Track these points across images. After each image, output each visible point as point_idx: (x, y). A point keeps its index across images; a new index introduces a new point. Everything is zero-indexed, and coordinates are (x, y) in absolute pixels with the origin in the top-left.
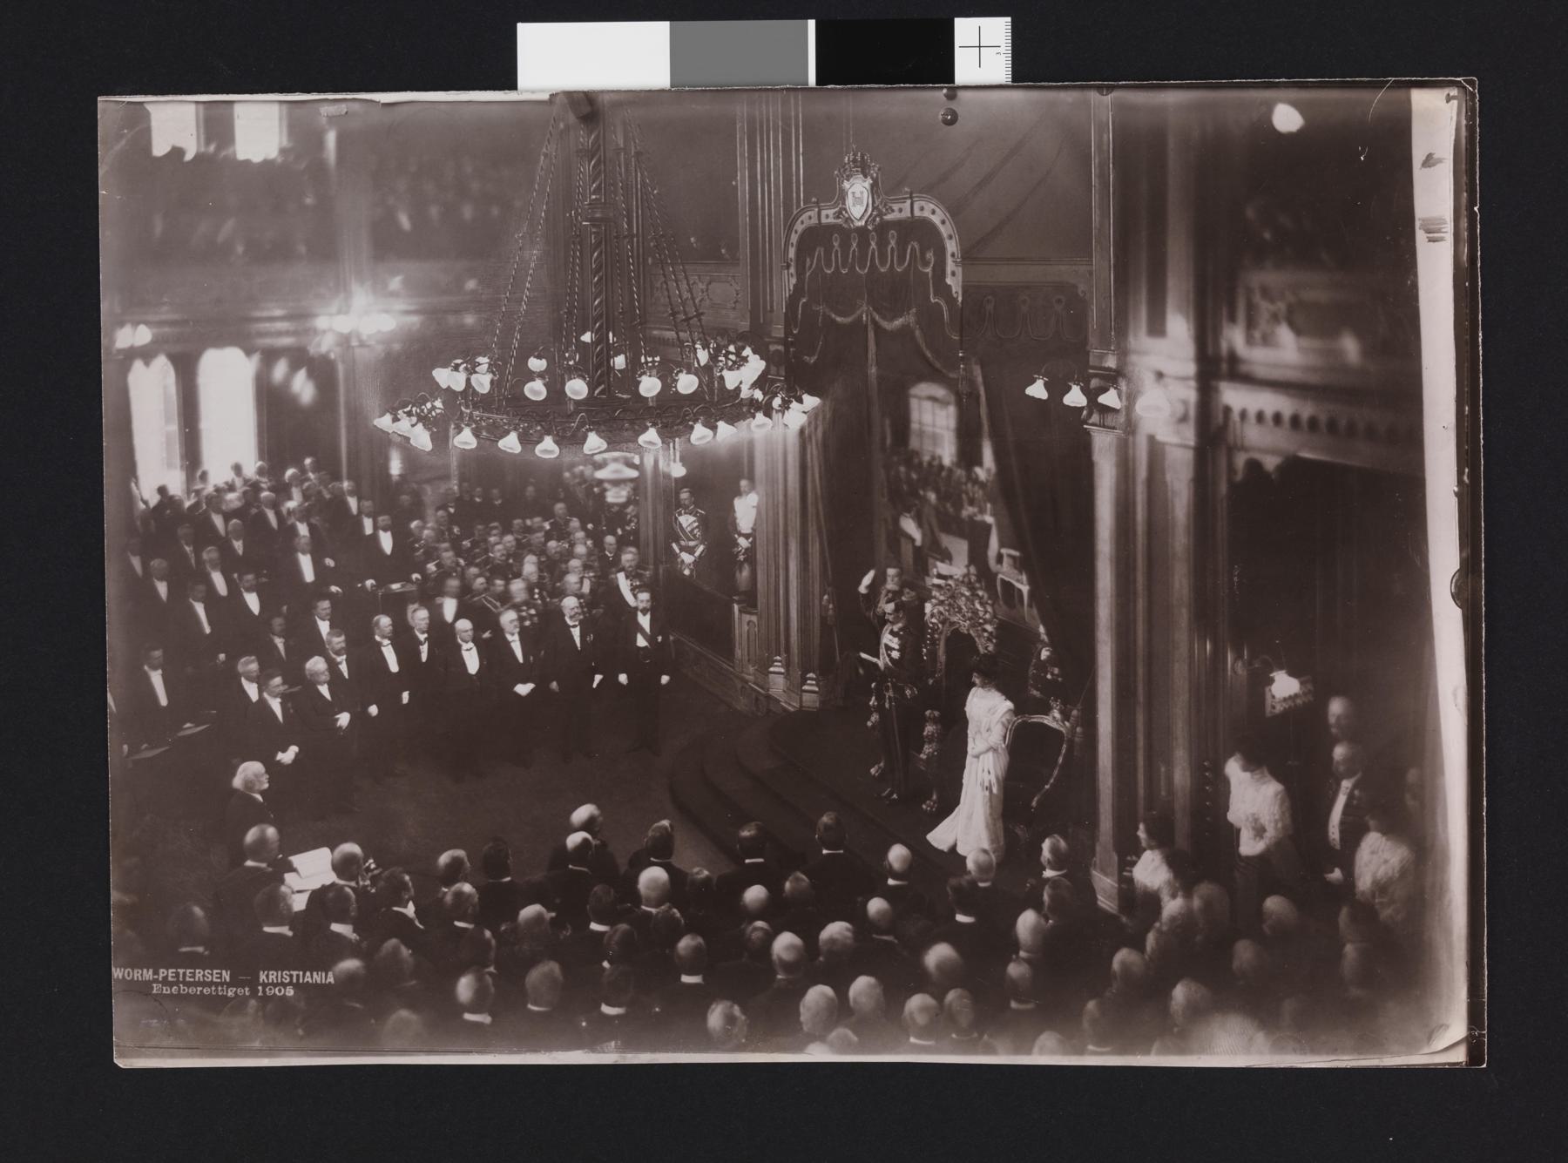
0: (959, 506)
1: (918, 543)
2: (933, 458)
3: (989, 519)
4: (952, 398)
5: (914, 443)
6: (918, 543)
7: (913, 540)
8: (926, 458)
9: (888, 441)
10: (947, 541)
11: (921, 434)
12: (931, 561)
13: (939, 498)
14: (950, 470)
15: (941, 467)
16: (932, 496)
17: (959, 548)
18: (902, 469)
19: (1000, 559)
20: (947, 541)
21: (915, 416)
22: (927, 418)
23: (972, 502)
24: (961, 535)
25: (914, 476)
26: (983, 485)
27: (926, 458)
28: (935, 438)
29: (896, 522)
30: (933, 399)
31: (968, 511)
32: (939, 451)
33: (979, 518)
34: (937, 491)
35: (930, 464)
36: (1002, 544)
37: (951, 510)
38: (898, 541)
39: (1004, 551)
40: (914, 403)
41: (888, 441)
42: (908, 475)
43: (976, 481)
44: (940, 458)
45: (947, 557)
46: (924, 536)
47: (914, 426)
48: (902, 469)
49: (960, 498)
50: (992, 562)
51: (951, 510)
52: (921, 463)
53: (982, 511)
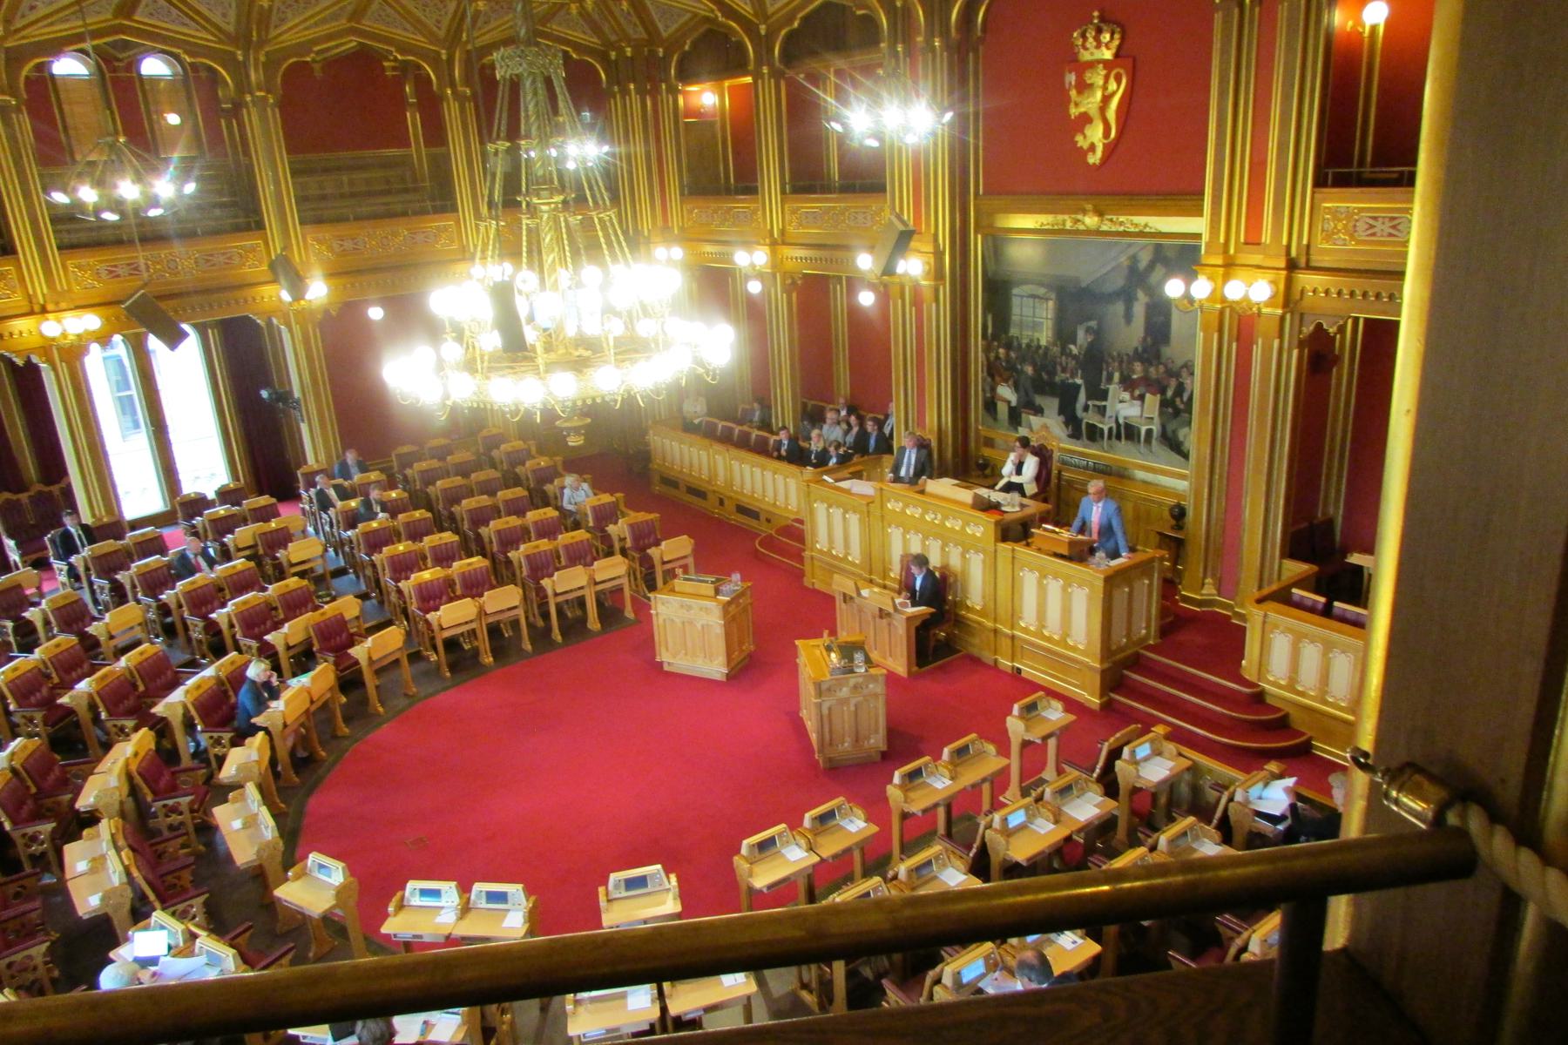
0: (1052, 373)
1: (1014, 404)
3: (1079, 381)
4: (1053, 296)
5: (1014, 331)
8: (1025, 342)
10: (1039, 400)
11: (1021, 325)
12: (1024, 416)
14: (1047, 348)
15: (1039, 347)
16: (1029, 370)
17: (1051, 404)
18: (1001, 351)
19: (1086, 408)
20: (1039, 400)
21: (1016, 310)
22: (1027, 311)
23: (1064, 370)
24: (1053, 394)
25: (1013, 355)
26: (1075, 357)
27: (1025, 342)
28: (1036, 326)
29: (993, 389)
30: (1034, 296)
31: (1060, 377)
32: (1037, 335)
34: (1034, 365)
35: (1028, 346)
36: (1089, 397)
40: (1015, 302)
42: (1007, 355)
43: (1070, 355)
45: (1039, 411)
46: (1019, 401)
48: (1001, 351)
50: (1080, 413)
52: (1020, 345)
53: (1073, 375)
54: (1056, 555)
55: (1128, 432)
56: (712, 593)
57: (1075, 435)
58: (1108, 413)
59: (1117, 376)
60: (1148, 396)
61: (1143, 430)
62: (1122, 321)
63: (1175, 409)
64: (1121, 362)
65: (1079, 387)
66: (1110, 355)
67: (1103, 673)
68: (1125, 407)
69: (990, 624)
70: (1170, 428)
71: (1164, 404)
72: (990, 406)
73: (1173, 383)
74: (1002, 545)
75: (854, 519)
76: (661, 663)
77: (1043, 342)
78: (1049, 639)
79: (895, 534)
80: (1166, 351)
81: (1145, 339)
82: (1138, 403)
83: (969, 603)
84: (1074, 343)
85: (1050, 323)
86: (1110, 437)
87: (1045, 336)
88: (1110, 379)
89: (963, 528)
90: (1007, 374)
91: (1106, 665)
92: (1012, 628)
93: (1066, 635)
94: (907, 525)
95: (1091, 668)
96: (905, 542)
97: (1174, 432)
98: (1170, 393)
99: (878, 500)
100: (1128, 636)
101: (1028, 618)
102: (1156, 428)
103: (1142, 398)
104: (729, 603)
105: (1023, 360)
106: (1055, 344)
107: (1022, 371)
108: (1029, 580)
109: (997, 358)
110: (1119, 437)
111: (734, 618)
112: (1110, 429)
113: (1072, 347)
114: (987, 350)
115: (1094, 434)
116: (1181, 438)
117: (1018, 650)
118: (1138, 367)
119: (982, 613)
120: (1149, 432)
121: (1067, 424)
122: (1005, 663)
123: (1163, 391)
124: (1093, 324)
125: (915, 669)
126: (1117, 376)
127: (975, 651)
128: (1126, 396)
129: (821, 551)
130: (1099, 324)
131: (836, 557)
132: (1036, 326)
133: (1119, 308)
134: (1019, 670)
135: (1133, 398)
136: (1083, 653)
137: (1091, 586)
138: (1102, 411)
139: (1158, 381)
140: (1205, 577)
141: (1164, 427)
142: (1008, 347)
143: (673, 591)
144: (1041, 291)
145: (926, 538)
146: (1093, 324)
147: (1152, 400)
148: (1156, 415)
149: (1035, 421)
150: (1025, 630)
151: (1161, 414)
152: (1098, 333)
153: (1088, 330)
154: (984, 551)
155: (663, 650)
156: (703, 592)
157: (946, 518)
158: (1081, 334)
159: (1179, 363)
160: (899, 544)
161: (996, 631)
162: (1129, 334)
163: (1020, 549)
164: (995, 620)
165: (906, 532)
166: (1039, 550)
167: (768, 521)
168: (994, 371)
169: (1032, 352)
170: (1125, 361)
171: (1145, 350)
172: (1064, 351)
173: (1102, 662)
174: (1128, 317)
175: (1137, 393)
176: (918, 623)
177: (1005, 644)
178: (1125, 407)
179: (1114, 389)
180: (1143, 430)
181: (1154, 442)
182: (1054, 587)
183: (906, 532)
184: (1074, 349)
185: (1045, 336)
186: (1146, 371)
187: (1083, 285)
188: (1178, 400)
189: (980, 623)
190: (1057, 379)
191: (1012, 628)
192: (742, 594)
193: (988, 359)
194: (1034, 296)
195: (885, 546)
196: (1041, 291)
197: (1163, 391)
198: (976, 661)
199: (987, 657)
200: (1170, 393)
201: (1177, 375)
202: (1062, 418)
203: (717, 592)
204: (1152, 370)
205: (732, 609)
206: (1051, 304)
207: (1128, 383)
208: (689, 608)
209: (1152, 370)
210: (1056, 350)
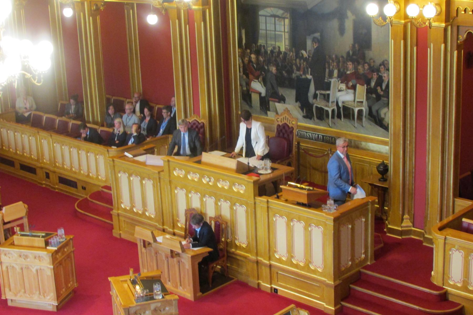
0: (290, 72)
1: (263, 94)
2: (274, 48)
3: (309, 77)
4: (288, 16)
5: (261, 42)
6: (263, 94)
7: (260, 94)
9: (244, 41)
10: (282, 91)
12: (271, 103)
13: (277, 69)
14: (285, 53)
15: (280, 52)
16: (273, 69)
17: (290, 94)
18: (253, 56)
19: (315, 96)
20: (282, 91)
21: (262, 26)
22: (270, 27)
23: (298, 69)
25: (261, 59)
26: (306, 60)
27: (269, 49)
28: (276, 38)
29: (248, 84)
30: (274, 16)
32: (278, 44)
33: (303, 77)
34: (277, 66)
35: (272, 52)
36: (316, 89)
37: (285, 74)
38: (250, 97)
39: (317, 92)
40: (262, 20)
41: (244, 41)
42: (257, 59)
44: (279, 47)
45: (282, 99)
46: (267, 91)
47: (262, 32)
48: (253, 56)
49: (291, 67)
50: (311, 100)
51: (285, 74)
52: (266, 52)
53: (305, 73)
54: (299, 204)
55: (345, 113)
56: (43, 245)
57: (308, 116)
58: (331, 100)
59: (336, 73)
60: (358, 85)
61: (356, 110)
62: (338, 33)
63: (377, 94)
64: (338, 65)
65: (310, 81)
66: (330, 57)
67: (336, 288)
68: (344, 95)
69: (254, 258)
70: (374, 109)
71: (369, 91)
72: (247, 96)
73: (375, 76)
74: (259, 199)
75: (149, 184)
76: (6, 300)
77: (283, 49)
78: (297, 266)
79: (181, 194)
80: (370, 54)
81: (354, 46)
82: (351, 91)
83: (237, 242)
84: (305, 50)
85: (287, 36)
86: (333, 117)
87: (283, 45)
88: (331, 75)
89: (230, 187)
90: (257, 73)
91: (338, 282)
92: (270, 259)
93: (308, 262)
94: (188, 187)
95: (328, 285)
96: (188, 200)
97: (377, 111)
98: (373, 84)
99: (166, 169)
100: (353, 260)
101: (281, 251)
102: (365, 109)
103: (354, 88)
104: (57, 252)
105: (268, 62)
106: (290, 50)
107: (268, 70)
108: (280, 224)
109: (250, 61)
110: (339, 117)
111: (60, 263)
112: (333, 111)
113: (304, 52)
114: (242, 56)
115: (321, 115)
116: (382, 116)
117: (275, 275)
118: (350, 65)
119: (247, 250)
120: (360, 112)
121: (302, 108)
122: (266, 285)
123: (368, 82)
124: (317, 35)
125: (199, 294)
126: (336, 73)
127: (243, 278)
128: (343, 86)
129: (125, 210)
130: (321, 36)
131: (137, 214)
132: (276, 38)
133: (335, 23)
134: (276, 290)
135: (348, 88)
136: (321, 274)
137: (325, 225)
138: (327, 98)
139: (364, 75)
140: (403, 214)
141: (370, 108)
142: (258, 53)
143: (13, 244)
144: (280, 12)
145: (203, 196)
146: (317, 35)
147: (361, 90)
148: (364, 100)
149: (279, 106)
150: (279, 260)
151: (368, 99)
152: (321, 42)
153: (314, 40)
154: (247, 204)
155: (7, 290)
156: (36, 244)
157: (217, 180)
158: (309, 43)
159: (378, 62)
160: (184, 202)
161: (257, 262)
162: (344, 43)
163: (273, 201)
164: (257, 254)
165: (188, 192)
166: (286, 201)
167: (84, 188)
168: (248, 71)
169: (275, 57)
170: (341, 62)
171: (354, 54)
172: (298, 55)
173: (335, 281)
174: (342, 30)
175: (351, 84)
176: (200, 260)
177: (265, 271)
178: (344, 95)
179: (334, 81)
180: (356, 110)
181: (364, 119)
182: (299, 227)
183: (188, 192)
184: (304, 52)
185: (283, 45)
186: (356, 68)
187: (309, 8)
188: (379, 88)
189: (245, 257)
190: (294, 75)
191: (270, 259)
192: (66, 244)
193: (243, 62)
194: (274, 16)
195: (173, 203)
196: (280, 12)
197: (368, 82)
198: (244, 286)
199: (253, 282)
200: (373, 84)
201: (378, 71)
202: (298, 104)
203: (47, 243)
204: (360, 67)
205: (59, 256)
206: (287, 21)
207: (343, 78)
208: (26, 257)
209: (360, 67)
210: (292, 54)
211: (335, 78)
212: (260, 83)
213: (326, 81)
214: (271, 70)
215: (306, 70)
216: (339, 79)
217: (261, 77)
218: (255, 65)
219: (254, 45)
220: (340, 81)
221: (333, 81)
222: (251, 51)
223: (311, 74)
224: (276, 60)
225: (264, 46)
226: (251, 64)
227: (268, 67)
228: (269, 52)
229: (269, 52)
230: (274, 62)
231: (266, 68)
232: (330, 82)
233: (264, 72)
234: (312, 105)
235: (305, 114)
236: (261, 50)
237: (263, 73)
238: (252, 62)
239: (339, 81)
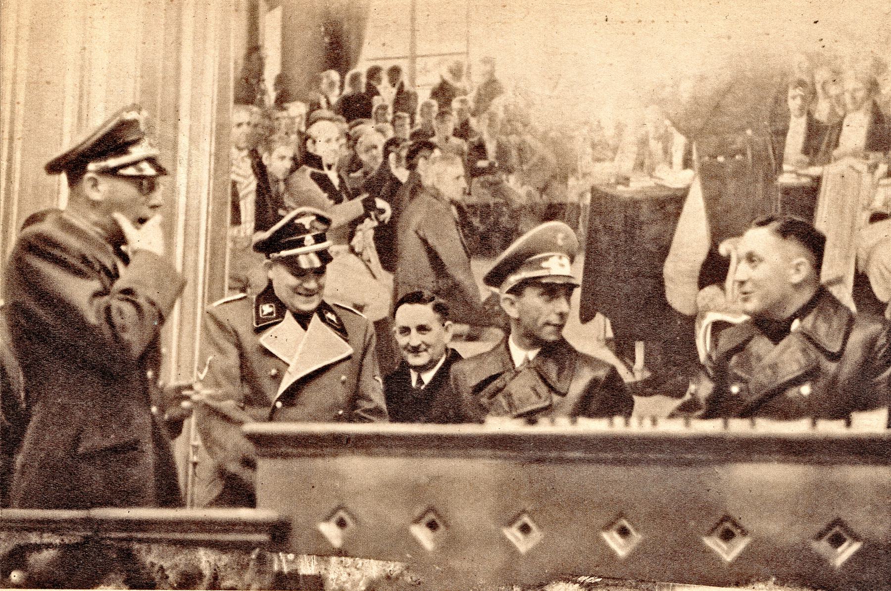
13: (473, 172)
107: (417, 187)
142: (355, 108)
211: (855, 154)
212: (357, 254)
213: (786, 179)
214: (428, 181)
215: (656, 146)
216: (874, 156)
217: (369, 225)
218: (333, 176)
219: (334, 75)
220: (883, 168)
221: (830, 172)
222: (315, 106)
223: (687, 163)
224: (463, 131)
225: (395, 72)
226: (310, 170)
227: (412, 167)
228: (424, 96)
229: (424, 96)
230: (456, 141)
231: (402, 174)
232: (818, 180)
233: (389, 198)
234: (691, 321)
235: (639, 377)
236: (372, 91)
237: (380, 203)
238: (313, 160)
239: (874, 167)
